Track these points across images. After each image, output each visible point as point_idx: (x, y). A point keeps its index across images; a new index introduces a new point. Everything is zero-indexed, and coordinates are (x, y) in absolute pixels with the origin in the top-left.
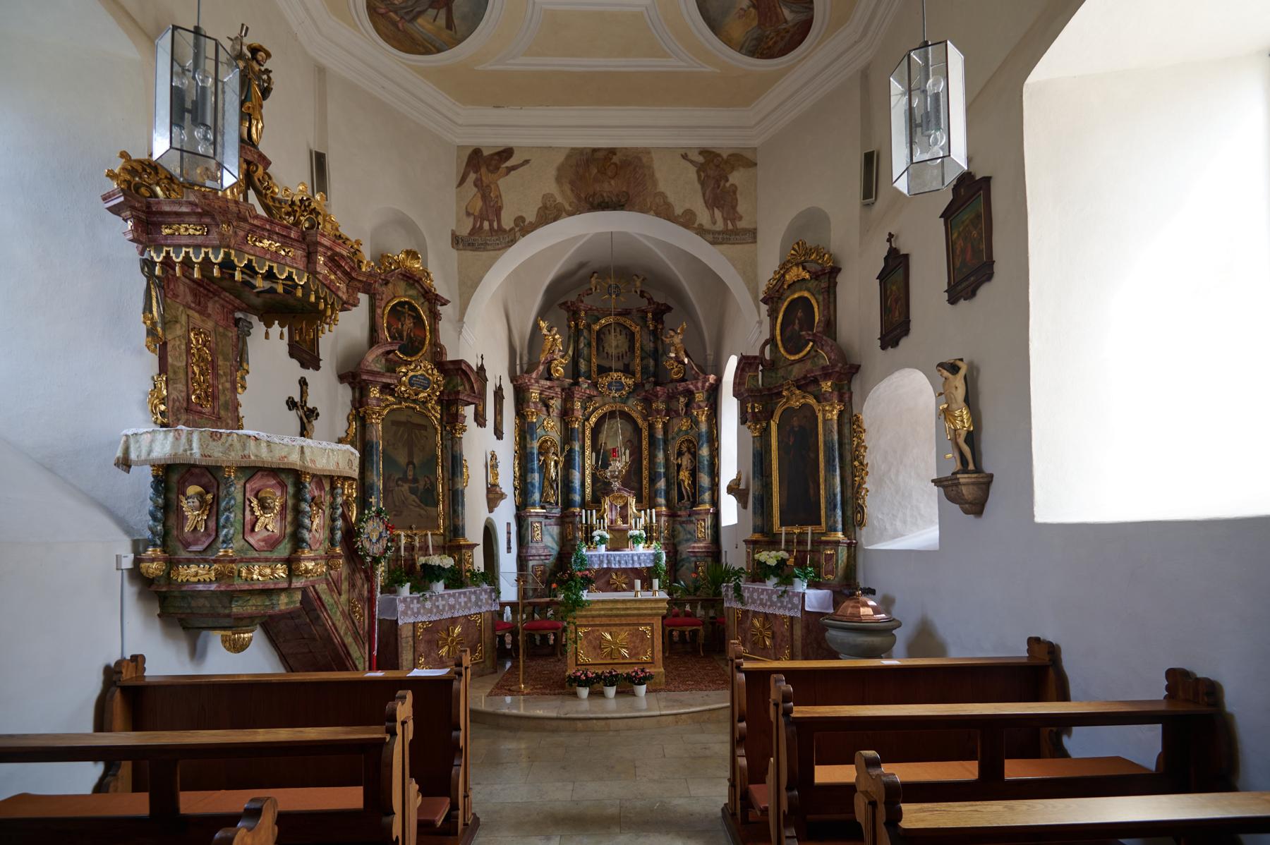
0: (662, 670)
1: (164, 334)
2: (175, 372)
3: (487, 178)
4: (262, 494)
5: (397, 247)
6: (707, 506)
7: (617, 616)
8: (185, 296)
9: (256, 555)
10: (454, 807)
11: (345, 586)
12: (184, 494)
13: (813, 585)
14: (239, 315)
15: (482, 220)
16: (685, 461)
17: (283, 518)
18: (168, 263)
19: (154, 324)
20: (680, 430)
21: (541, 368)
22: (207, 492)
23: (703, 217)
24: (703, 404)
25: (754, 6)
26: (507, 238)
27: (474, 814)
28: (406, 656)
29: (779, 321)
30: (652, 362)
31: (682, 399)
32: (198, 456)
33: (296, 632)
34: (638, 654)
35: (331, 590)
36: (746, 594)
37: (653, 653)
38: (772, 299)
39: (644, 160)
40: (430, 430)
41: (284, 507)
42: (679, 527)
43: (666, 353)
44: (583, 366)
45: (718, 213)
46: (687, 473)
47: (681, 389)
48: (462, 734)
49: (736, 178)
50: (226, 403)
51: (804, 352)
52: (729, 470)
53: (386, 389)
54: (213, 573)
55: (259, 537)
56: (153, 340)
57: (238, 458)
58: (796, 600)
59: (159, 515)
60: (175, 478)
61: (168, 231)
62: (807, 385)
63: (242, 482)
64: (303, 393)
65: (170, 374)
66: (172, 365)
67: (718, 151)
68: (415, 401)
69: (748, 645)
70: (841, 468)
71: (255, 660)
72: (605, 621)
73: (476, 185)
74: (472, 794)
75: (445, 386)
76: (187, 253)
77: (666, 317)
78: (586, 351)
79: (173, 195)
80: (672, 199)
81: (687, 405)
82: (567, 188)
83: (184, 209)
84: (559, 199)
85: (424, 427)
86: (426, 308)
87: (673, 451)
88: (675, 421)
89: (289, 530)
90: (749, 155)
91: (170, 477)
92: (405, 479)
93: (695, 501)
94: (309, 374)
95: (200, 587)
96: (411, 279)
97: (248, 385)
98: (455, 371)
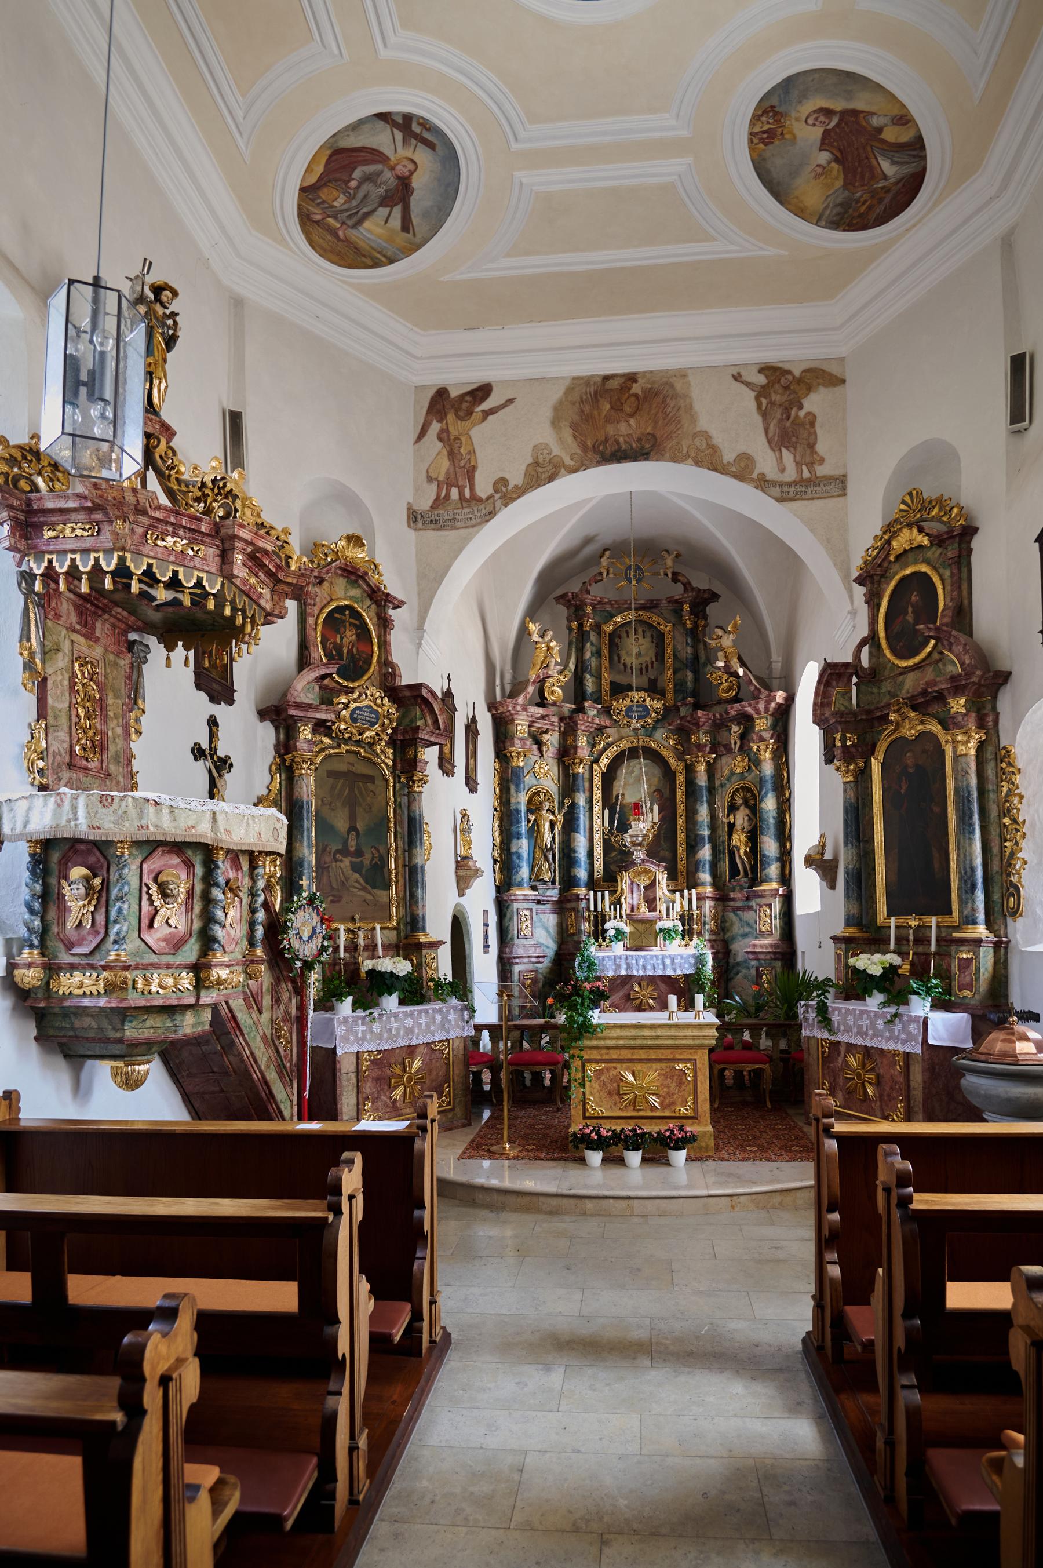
1: (43, 668)
2: (56, 717)
3: (455, 427)
4: (162, 878)
5: (333, 532)
7: (642, 1047)
8: (69, 614)
9: (154, 959)
10: (417, 1316)
11: (267, 1001)
12: (66, 878)
13: (941, 1004)
14: (133, 636)
15: (449, 486)
16: (741, 818)
17: (190, 909)
18: (50, 575)
19: (32, 655)
20: (733, 774)
21: (531, 689)
22: (95, 876)
23: (766, 462)
24: (766, 735)
25: (837, 160)
26: (483, 509)
27: (443, 1328)
28: (347, 1100)
30: (690, 675)
31: (735, 728)
32: (84, 828)
33: (205, 1066)
35: (249, 1007)
36: (836, 1018)
38: (871, 577)
39: (678, 386)
40: (379, 782)
41: (190, 894)
42: (731, 915)
43: (710, 660)
44: (590, 685)
45: (787, 456)
46: (743, 837)
47: (733, 713)
48: (427, 1214)
49: (814, 403)
50: (117, 756)
51: (922, 656)
53: (321, 727)
54: (102, 983)
55: (159, 935)
56: (31, 676)
57: (134, 829)
58: (914, 1028)
59: (37, 906)
60: (55, 857)
61: (51, 534)
62: (927, 704)
63: (138, 861)
64: (213, 737)
65: (50, 718)
66: (53, 708)
67: (786, 367)
68: (358, 743)
70: (984, 829)
71: (153, 1102)
72: (626, 1054)
73: (440, 439)
74: (440, 1300)
75: (399, 720)
76: (73, 560)
77: (712, 609)
78: (594, 663)
79: (58, 485)
80: (718, 439)
81: (743, 737)
82: (567, 434)
83: (71, 504)
84: (556, 451)
85: (371, 779)
86: (373, 614)
87: (722, 803)
88: (724, 760)
89: (197, 925)
90: (834, 369)
91: (51, 856)
92: (345, 852)
93: (755, 877)
94: (220, 711)
95: (86, 1002)
96: (353, 574)
97: (144, 729)
98: (411, 699)
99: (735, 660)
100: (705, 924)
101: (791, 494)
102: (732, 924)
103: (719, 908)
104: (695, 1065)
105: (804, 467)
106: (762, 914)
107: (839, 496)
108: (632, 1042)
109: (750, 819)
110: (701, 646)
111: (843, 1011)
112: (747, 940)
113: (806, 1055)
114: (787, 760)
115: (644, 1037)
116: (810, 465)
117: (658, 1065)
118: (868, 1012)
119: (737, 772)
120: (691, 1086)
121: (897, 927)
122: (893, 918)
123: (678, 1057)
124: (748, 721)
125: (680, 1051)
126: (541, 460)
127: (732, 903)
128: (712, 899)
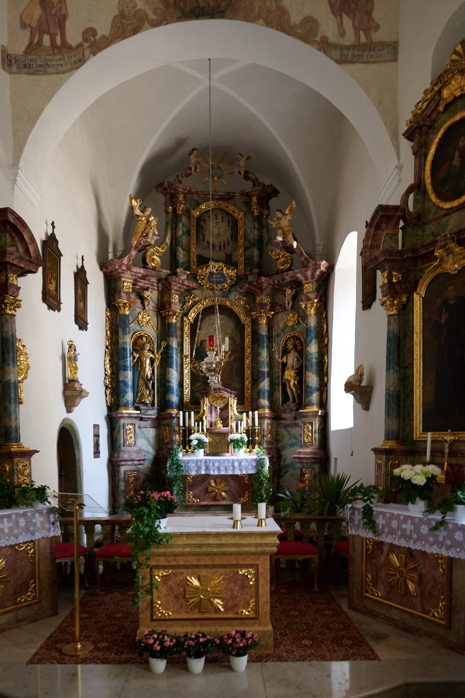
0: (270, 628)
6: (315, 408)
7: (207, 554)
16: (291, 359)
20: (286, 326)
23: (328, 27)
24: (312, 296)
29: (430, 158)
30: (256, 252)
31: (289, 291)
34: (236, 606)
36: (380, 521)
37: (257, 602)
38: (418, 132)
42: (283, 430)
45: (347, 22)
46: (292, 373)
47: (288, 279)
52: (343, 364)
69: (382, 587)
77: (273, 203)
81: (295, 298)
87: (277, 348)
88: (280, 316)
93: (301, 402)
99: (291, 236)
100: (263, 436)
101: (350, 57)
102: (283, 437)
103: (274, 425)
104: (257, 570)
105: (362, 33)
106: (306, 430)
107: (390, 61)
108: (198, 550)
109: (298, 360)
110: (265, 230)
111: (388, 515)
112: (294, 449)
113: (351, 550)
114: (326, 316)
115: (210, 545)
116: (367, 31)
117: (223, 571)
118: (413, 518)
119: (289, 325)
120: (253, 590)
121: (433, 441)
122: (429, 435)
123: (241, 562)
124: (298, 287)
125: (243, 557)
126: (126, 13)
127: (283, 422)
128: (269, 418)
